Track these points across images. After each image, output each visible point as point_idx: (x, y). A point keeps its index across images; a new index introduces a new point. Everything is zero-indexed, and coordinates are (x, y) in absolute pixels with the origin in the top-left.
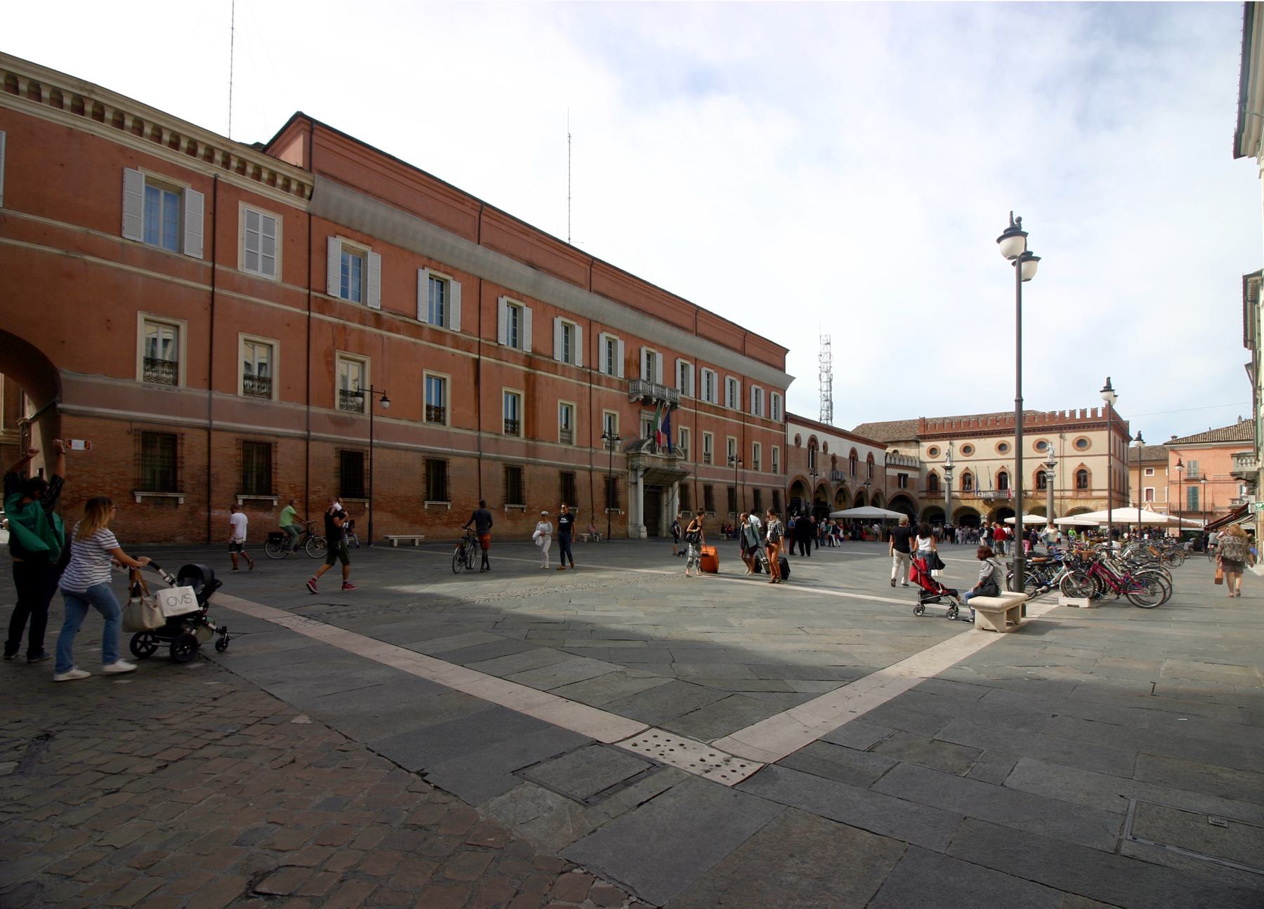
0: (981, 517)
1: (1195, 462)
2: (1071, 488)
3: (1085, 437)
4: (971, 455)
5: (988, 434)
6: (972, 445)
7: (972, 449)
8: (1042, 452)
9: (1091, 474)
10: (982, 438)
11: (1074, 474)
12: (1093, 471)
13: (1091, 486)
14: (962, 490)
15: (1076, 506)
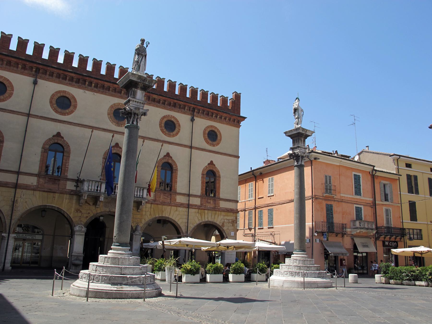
0: (77, 228)
1: (330, 177)
2: (199, 193)
3: (216, 128)
4: (69, 114)
5: (103, 87)
6: (73, 97)
7: (73, 103)
8: (169, 136)
9: (220, 177)
10: (92, 90)
11: (203, 174)
12: (222, 174)
13: (219, 194)
14: (43, 173)
15: (203, 220)
